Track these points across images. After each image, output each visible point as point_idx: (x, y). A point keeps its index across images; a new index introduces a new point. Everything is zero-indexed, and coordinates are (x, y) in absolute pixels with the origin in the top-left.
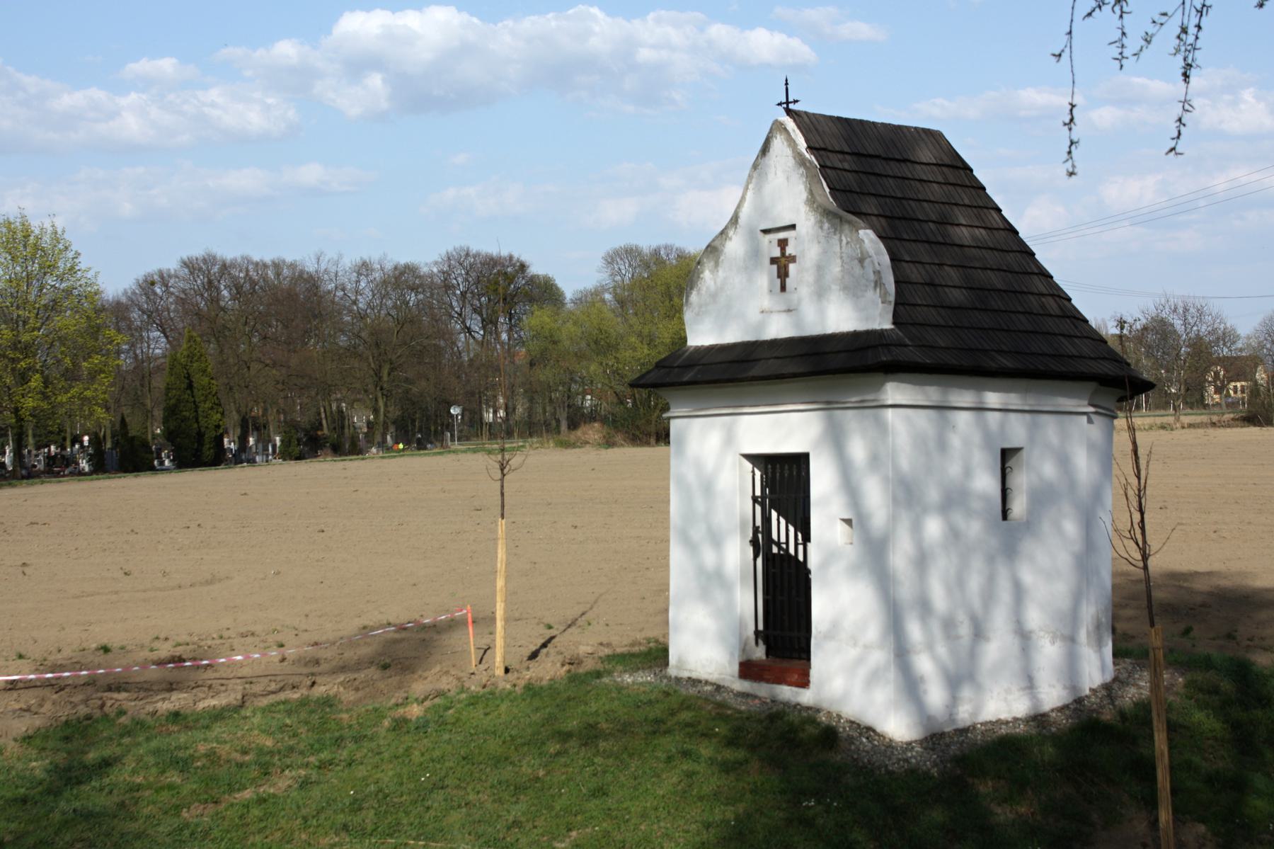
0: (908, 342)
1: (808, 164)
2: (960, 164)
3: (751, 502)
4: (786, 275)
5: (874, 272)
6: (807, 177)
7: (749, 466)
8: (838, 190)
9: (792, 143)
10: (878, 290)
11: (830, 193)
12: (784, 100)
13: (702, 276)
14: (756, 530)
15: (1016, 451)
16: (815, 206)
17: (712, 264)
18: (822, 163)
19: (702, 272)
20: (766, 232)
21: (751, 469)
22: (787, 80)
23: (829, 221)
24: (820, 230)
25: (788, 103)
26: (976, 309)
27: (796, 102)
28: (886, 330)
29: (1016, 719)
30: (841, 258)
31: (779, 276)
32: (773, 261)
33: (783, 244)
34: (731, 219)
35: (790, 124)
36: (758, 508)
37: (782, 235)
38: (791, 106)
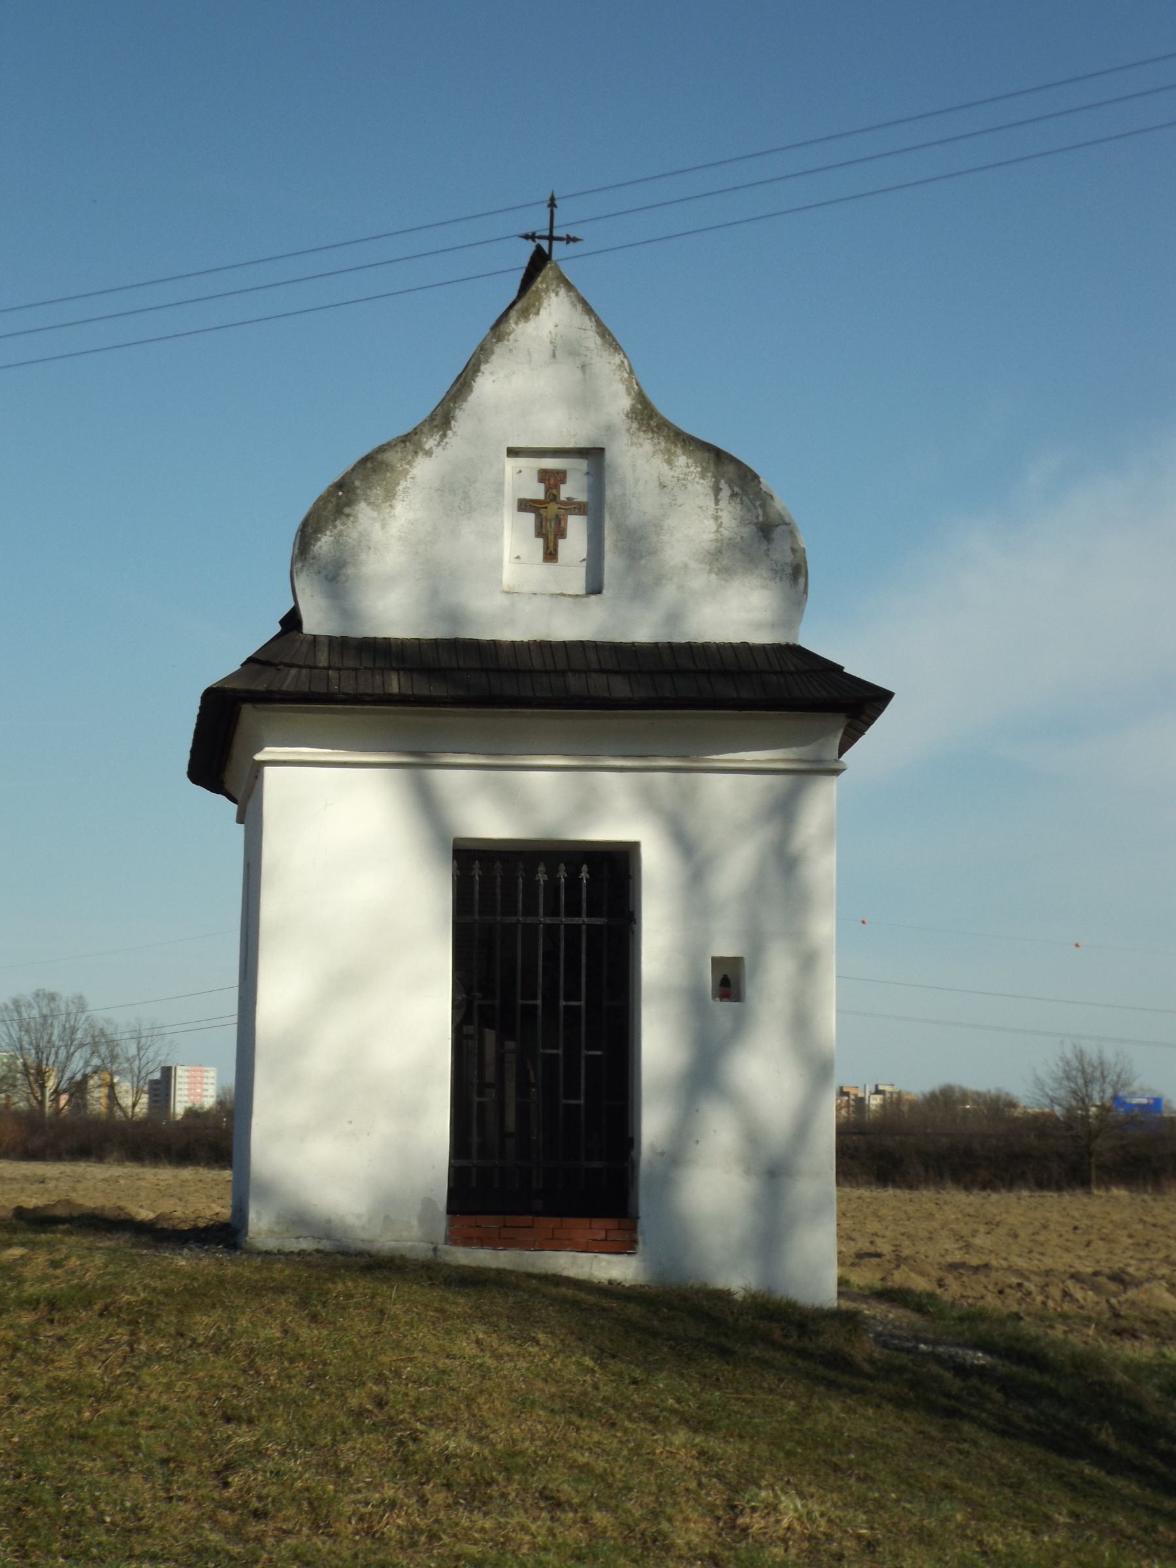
13: (347, 510)
19: (349, 503)
20: (513, 452)
24: (666, 467)
27: (569, 239)
30: (716, 518)
31: (540, 532)
33: (551, 479)
34: (432, 418)
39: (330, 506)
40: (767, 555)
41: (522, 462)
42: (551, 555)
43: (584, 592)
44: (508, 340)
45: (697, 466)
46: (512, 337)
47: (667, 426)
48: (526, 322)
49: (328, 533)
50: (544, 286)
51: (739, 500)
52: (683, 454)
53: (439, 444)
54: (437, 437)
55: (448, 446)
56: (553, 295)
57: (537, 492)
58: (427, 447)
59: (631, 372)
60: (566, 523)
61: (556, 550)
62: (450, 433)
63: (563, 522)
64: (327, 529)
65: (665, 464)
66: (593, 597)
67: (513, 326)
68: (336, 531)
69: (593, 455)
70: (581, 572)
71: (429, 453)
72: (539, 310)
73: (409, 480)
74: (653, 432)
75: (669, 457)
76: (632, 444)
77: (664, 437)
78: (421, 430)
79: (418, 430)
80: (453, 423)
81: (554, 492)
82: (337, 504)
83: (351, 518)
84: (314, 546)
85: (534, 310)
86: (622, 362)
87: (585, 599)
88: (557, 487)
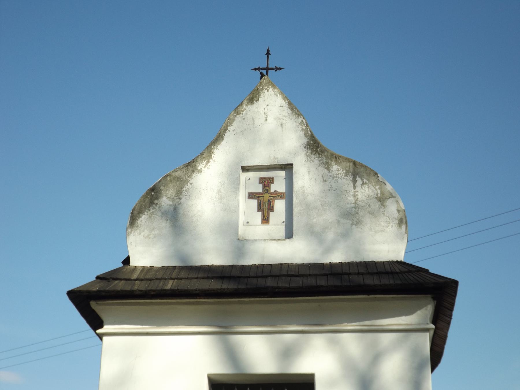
10: (404, 227)
13: (156, 202)
19: (157, 198)
20: (245, 169)
24: (326, 171)
27: (277, 69)
31: (260, 208)
33: (266, 182)
39: (147, 200)
40: (384, 214)
41: (250, 174)
42: (266, 220)
43: (284, 238)
44: (242, 114)
45: (343, 170)
46: (244, 113)
47: (326, 151)
48: (251, 105)
49: (146, 213)
50: (261, 87)
51: (367, 186)
52: (336, 165)
53: (205, 166)
54: (205, 163)
55: (210, 167)
56: (266, 91)
57: (259, 189)
58: (199, 168)
59: (307, 125)
60: (274, 204)
61: (268, 218)
62: (211, 160)
63: (272, 204)
64: (145, 211)
65: (326, 170)
66: (288, 240)
67: (245, 107)
68: (150, 212)
69: (288, 168)
70: (283, 228)
72: (258, 99)
73: (189, 185)
74: (319, 154)
75: (328, 166)
76: (308, 161)
77: (325, 156)
78: (196, 160)
79: (195, 160)
80: (213, 155)
81: (267, 188)
82: (151, 199)
83: (158, 206)
84: (138, 220)
85: (256, 99)
86: (302, 121)
87: (284, 241)
88: (269, 186)
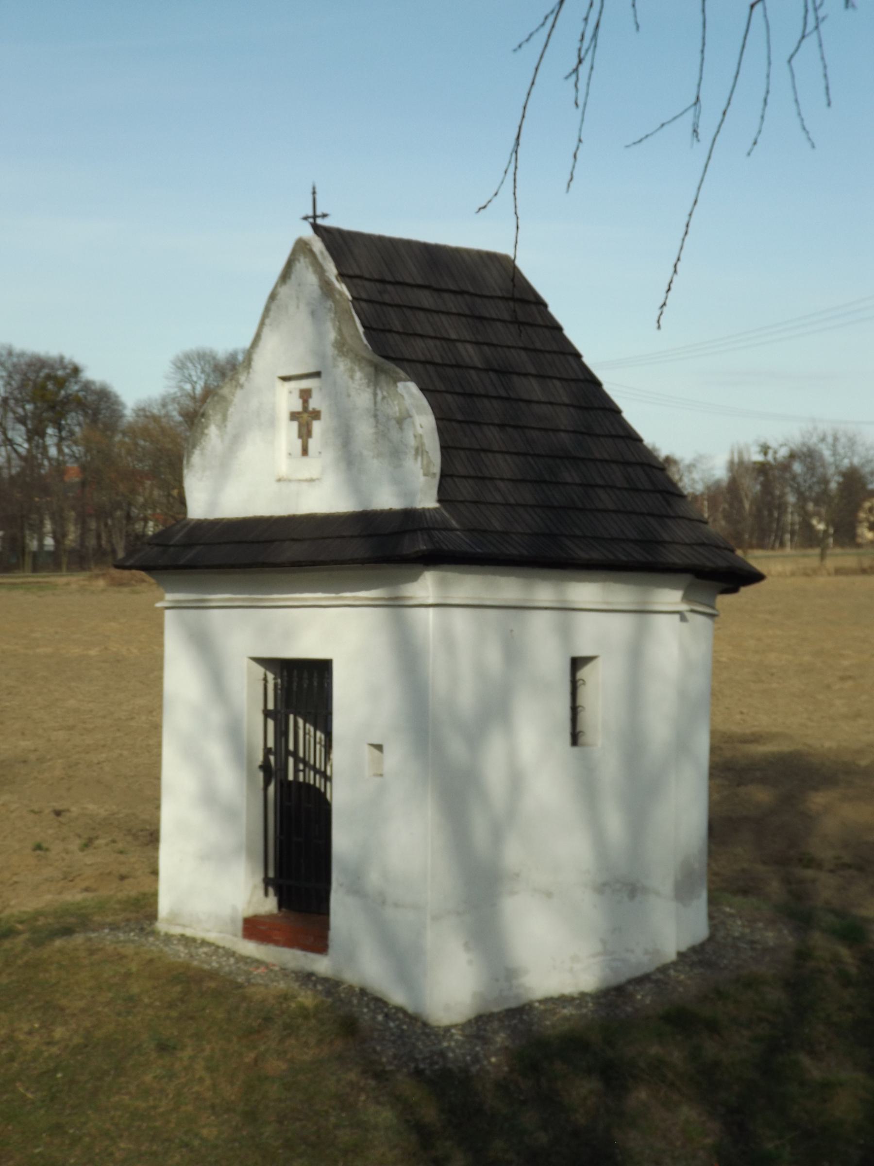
0: (454, 524)
1: (338, 297)
2: (532, 298)
3: (260, 717)
4: (309, 434)
5: (415, 436)
6: (336, 313)
7: (260, 670)
8: (374, 330)
9: (320, 271)
10: (419, 459)
11: (365, 334)
12: (311, 213)
13: (206, 431)
14: (267, 751)
15: (587, 660)
16: (345, 349)
17: (219, 417)
18: (356, 296)
19: (207, 427)
20: (285, 379)
21: (262, 676)
22: (314, 188)
23: (361, 369)
25: (315, 217)
26: (545, 482)
27: (324, 216)
28: (429, 510)
29: (583, 995)
31: (300, 436)
32: (294, 416)
33: (305, 395)
35: (318, 246)
36: (271, 723)
37: (305, 384)
38: (320, 221)
62: (251, 371)
71: (242, 386)
